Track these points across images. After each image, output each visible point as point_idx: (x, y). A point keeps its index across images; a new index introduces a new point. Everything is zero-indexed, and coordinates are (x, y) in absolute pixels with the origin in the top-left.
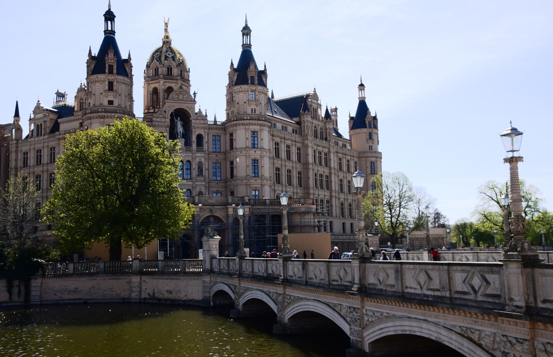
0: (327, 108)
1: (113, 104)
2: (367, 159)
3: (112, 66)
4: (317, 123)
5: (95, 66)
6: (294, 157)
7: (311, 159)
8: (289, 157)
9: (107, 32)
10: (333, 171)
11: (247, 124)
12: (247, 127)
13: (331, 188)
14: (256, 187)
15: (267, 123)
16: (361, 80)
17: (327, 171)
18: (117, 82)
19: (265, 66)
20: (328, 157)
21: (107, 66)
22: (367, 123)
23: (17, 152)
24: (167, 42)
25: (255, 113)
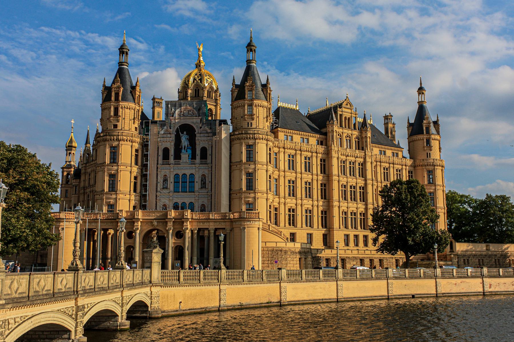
0: (365, 116)
1: (117, 128)
2: (424, 167)
3: (118, 93)
4: (350, 132)
5: (106, 95)
6: (316, 167)
7: (335, 171)
8: (308, 168)
9: (120, 64)
10: (369, 182)
11: (242, 138)
12: (243, 141)
13: (367, 200)
14: (249, 201)
15: (264, 136)
16: (421, 84)
17: (361, 182)
18: (122, 108)
19: (268, 79)
20: (364, 167)
22: (424, 128)
23: (85, 173)
25: (251, 126)
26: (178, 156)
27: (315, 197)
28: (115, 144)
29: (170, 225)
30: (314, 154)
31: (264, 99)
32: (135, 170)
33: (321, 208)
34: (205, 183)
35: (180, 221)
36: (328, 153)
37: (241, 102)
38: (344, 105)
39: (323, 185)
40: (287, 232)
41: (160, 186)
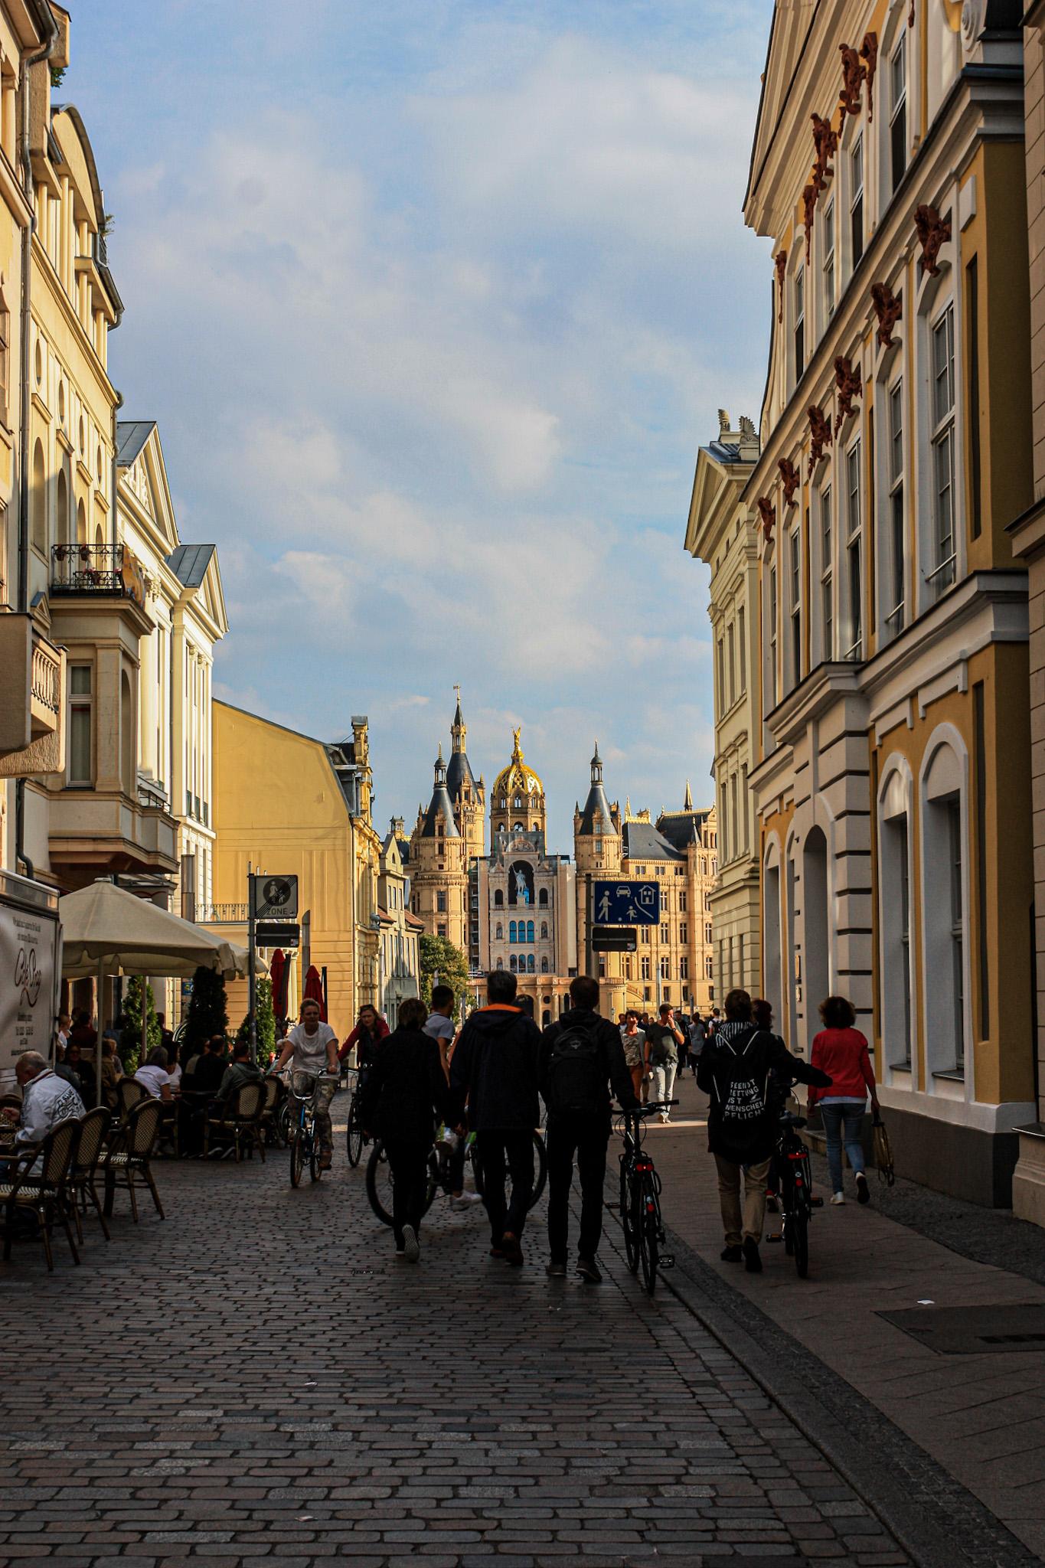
21: (437, 828)
24: (515, 760)
26: (513, 900)
27: (673, 941)
28: (443, 888)
29: (539, 990)
30: (672, 888)
31: (614, 832)
32: (464, 917)
33: (680, 956)
34: (546, 932)
35: (549, 986)
36: (689, 884)
37: (588, 837)
38: (709, 817)
39: (684, 925)
40: (640, 986)
41: (493, 936)
